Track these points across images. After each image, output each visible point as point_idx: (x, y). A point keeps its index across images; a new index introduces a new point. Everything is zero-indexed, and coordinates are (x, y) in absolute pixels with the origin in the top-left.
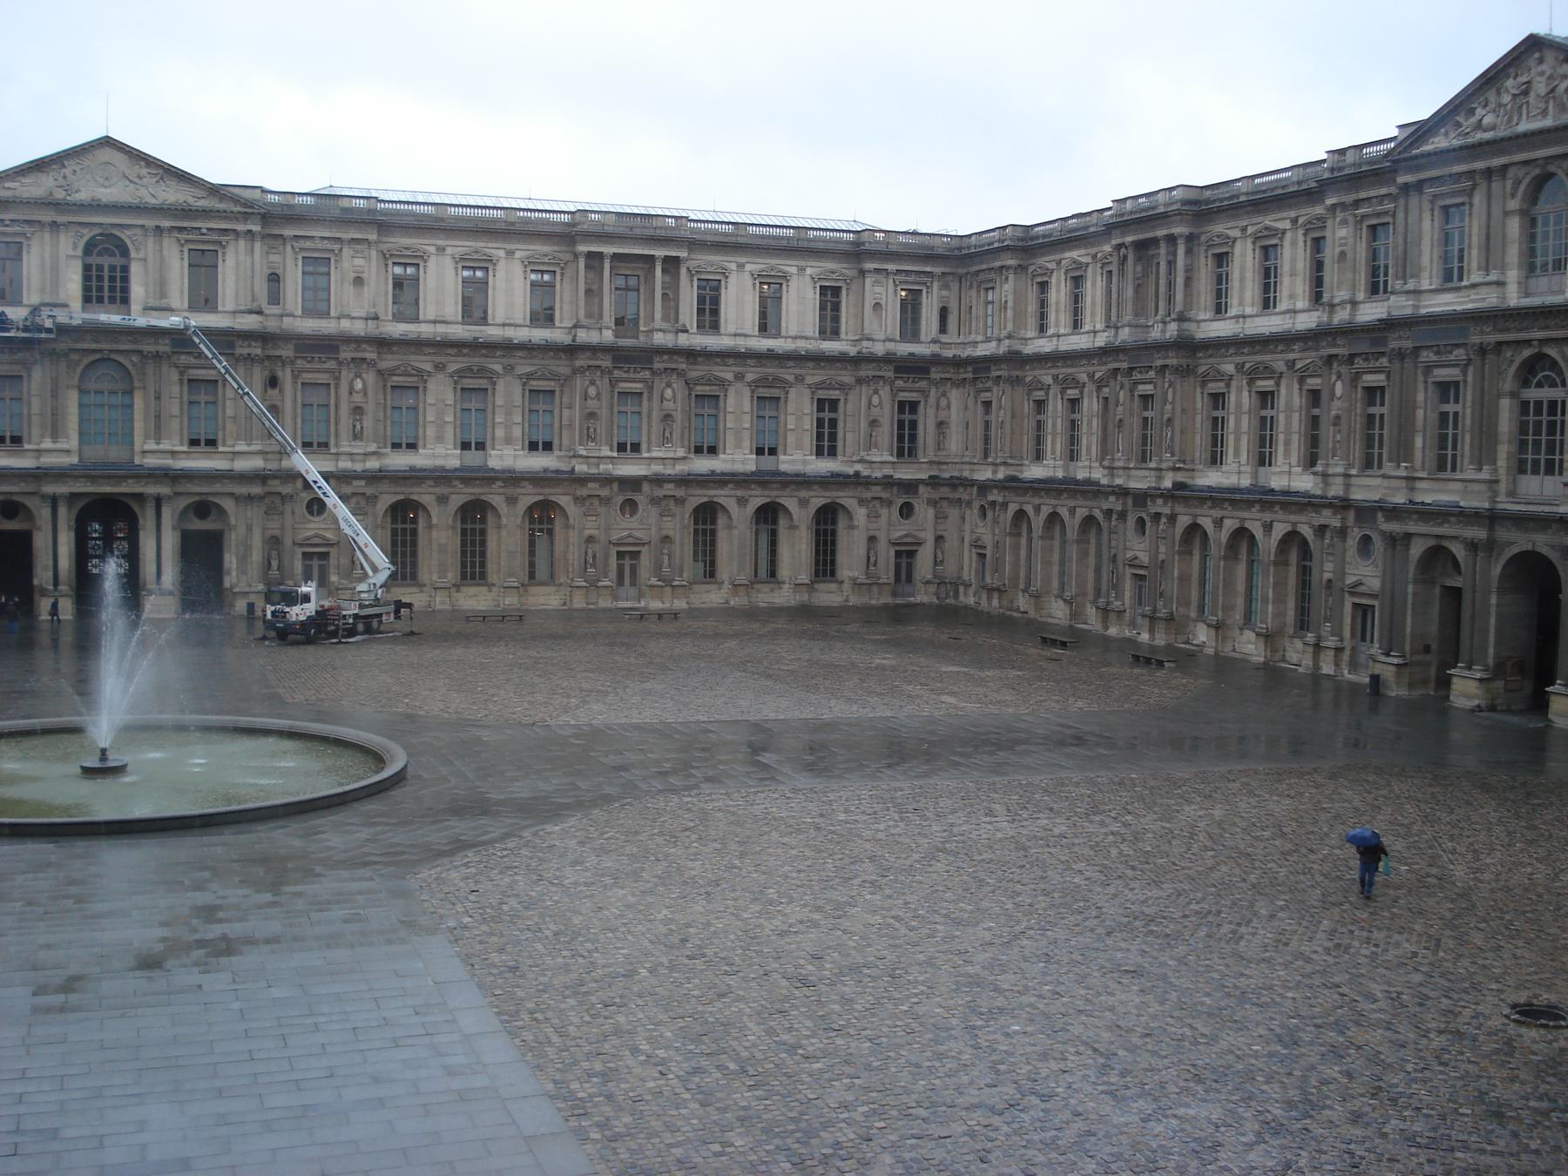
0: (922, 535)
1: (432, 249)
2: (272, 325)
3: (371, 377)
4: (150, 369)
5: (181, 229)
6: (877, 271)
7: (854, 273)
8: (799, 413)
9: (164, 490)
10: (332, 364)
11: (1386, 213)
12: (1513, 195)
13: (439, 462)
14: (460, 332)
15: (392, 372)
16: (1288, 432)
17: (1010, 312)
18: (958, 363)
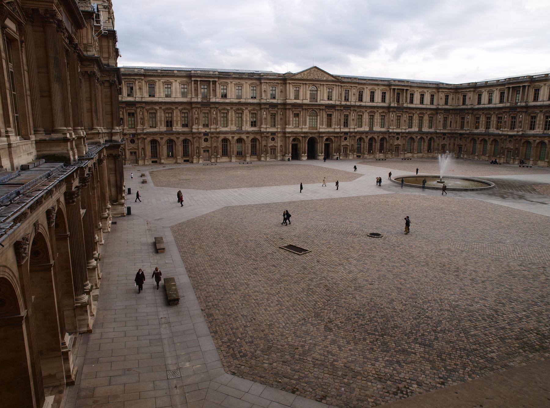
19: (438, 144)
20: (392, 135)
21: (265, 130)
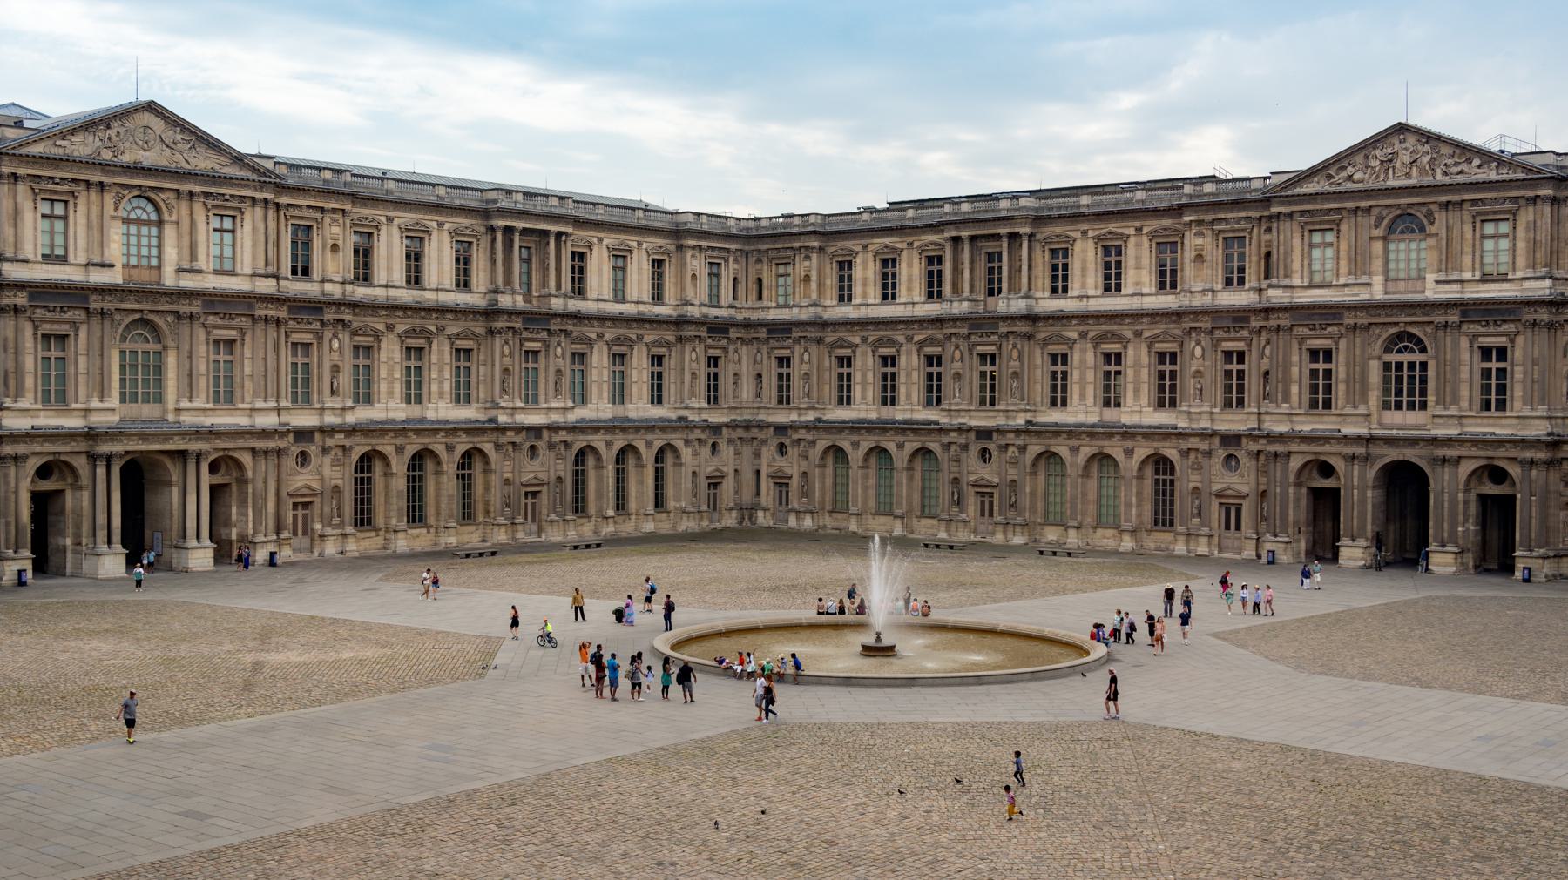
4: (185, 329)
5: (207, 195)
7: (673, 248)
11: (1243, 230)
12: (1377, 227)
13: (391, 415)
16: (1137, 381)
17: (814, 285)
18: (748, 325)
20: (510, 436)
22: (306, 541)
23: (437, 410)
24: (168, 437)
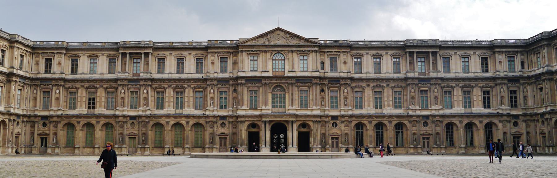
0: (522, 131)
1: (365, 53)
2: (322, 75)
3: (349, 89)
5: (298, 51)
6: (499, 52)
7: (492, 53)
8: (477, 95)
9: (294, 119)
10: (338, 85)
13: (369, 112)
14: (374, 76)
15: (355, 87)
17: (546, 59)
18: (529, 78)
19: (505, 133)
21: (211, 114)
22: (337, 149)
23: (387, 110)
24: (282, 116)
